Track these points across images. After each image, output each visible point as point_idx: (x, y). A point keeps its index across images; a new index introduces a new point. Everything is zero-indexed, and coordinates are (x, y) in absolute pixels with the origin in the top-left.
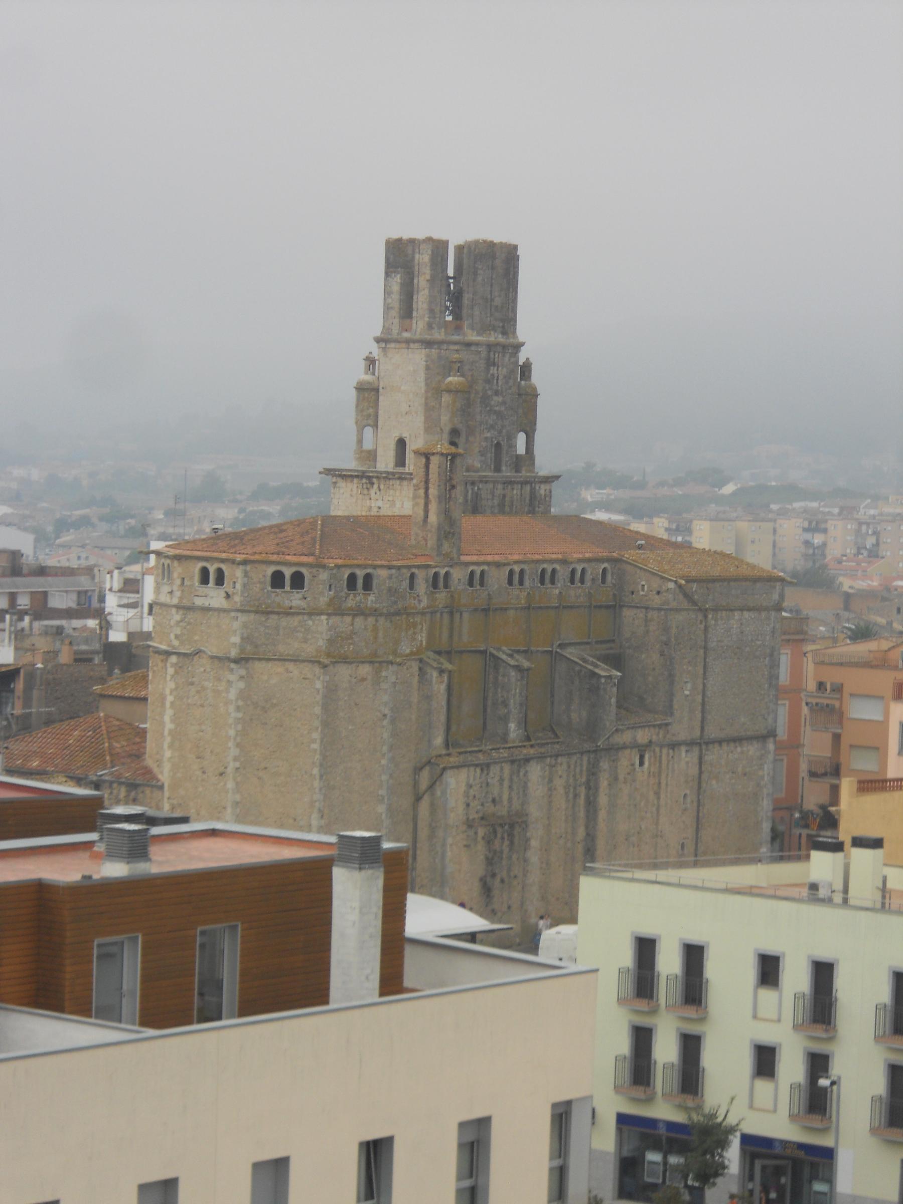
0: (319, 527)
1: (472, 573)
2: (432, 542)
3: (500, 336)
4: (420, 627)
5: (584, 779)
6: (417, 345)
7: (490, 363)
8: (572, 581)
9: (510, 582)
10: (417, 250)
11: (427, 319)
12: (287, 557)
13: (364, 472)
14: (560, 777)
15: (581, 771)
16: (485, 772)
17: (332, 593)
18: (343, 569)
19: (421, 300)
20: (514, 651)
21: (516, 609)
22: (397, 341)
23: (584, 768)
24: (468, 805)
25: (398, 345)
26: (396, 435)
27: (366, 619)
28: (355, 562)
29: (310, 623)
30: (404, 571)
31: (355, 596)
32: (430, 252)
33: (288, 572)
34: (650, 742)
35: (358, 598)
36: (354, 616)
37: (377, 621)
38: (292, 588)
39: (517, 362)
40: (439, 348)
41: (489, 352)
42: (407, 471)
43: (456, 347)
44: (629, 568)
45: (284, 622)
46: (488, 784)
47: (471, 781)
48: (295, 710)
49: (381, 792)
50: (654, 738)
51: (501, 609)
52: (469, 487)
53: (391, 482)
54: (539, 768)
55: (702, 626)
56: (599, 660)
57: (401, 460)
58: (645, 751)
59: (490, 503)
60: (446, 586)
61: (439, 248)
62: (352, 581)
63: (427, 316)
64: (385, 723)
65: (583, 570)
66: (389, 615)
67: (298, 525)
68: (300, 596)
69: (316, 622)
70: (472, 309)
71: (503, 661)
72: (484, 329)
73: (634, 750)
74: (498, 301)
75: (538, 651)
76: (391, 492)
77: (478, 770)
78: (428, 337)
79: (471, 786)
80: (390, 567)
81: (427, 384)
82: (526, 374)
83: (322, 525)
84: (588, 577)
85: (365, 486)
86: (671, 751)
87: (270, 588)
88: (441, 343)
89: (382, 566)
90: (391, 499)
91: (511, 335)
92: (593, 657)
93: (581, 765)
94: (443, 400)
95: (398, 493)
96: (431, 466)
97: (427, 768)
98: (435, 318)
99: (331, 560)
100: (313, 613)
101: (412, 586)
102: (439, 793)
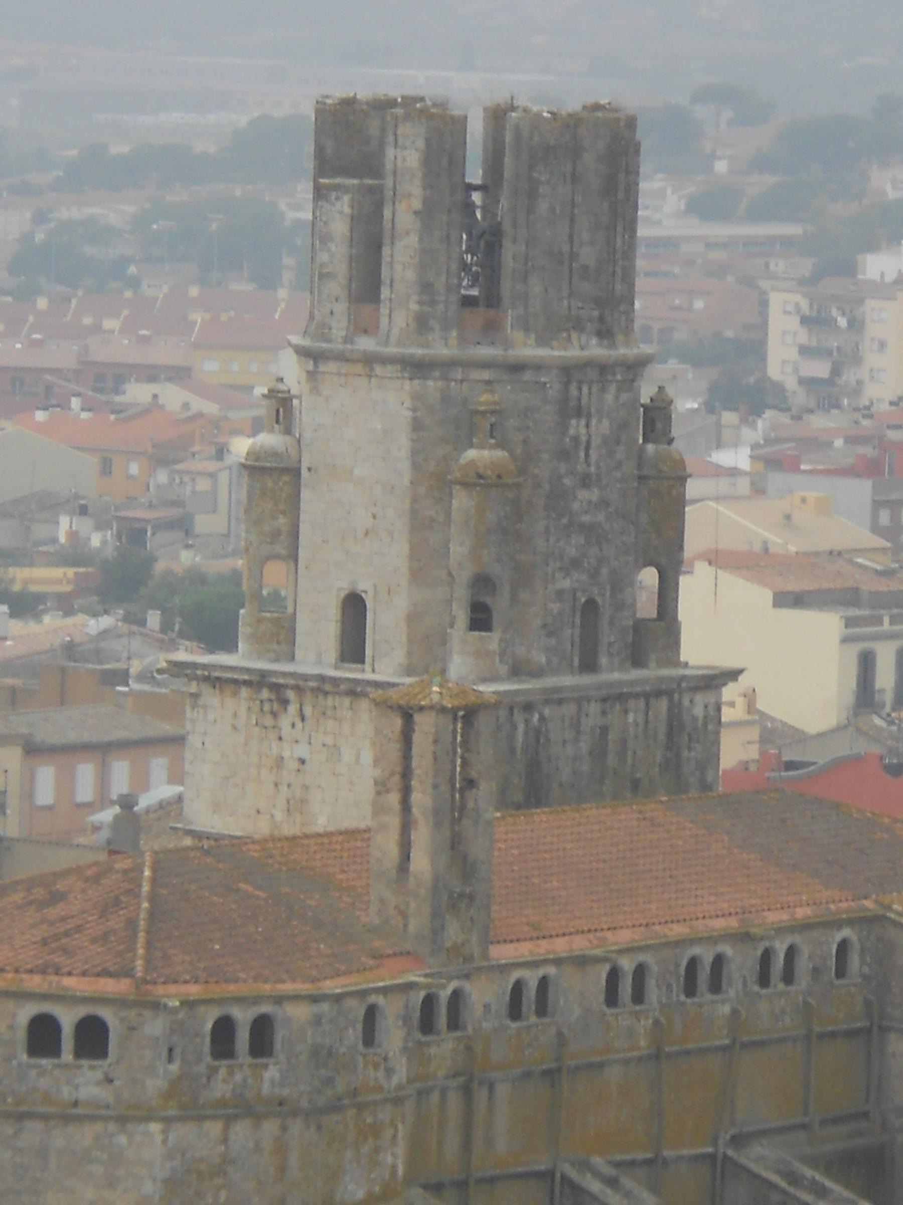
0: (146, 888)
1: (518, 988)
2: (418, 923)
3: (594, 341)
4: (389, 1133)
6: (391, 370)
7: (571, 410)
8: (764, 980)
9: (612, 999)
10: (391, 138)
11: (414, 307)
12: (68, 982)
13: (263, 674)
17: (174, 1068)
18: (202, 1009)
19: (402, 259)
20: (618, 1165)
21: (626, 1062)
22: (341, 357)
25: (345, 368)
26: (341, 585)
28: (232, 989)
29: (123, 1139)
30: (352, 1003)
31: (231, 1072)
32: (421, 144)
33: (68, 1019)
35: (238, 1077)
36: (229, 1120)
37: (284, 1128)
38: (79, 1052)
39: (636, 399)
40: (446, 378)
41: (567, 384)
42: (369, 676)
43: (486, 375)
45: (60, 1138)
51: (590, 1066)
52: (519, 717)
53: (330, 701)
56: (828, 1171)
57: (353, 647)
59: (570, 750)
60: (454, 1023)
61: (442, 130)
62: (224, 1030)
63: (415, 298)
65: (791, 952)
67: (96, 879)
68: (98, 1075)
69: (138, 1138)
70: (525, 278)
71: (594, 1197)
72: (551, 329)
74: (588, 255)
75: (680, 1158)
76: (331, 724)
78: (419, 352)
80: (314, 999)
81: (415, 466)
82: (659, 425)
83: (154, 881)
84: (803, 965)
85: (267, 707)
87: (24, 1057)
88: (452, 364)
89: (296, 998)
90: (329, 740)
91: (620, 338)
92: (812, 1162)
94: (455, 503)
95: (346, 729)
96: (417, 738)
98: (433, 303)
99: (172, 989)
100: (129, 1115)
101: (369, 1037)
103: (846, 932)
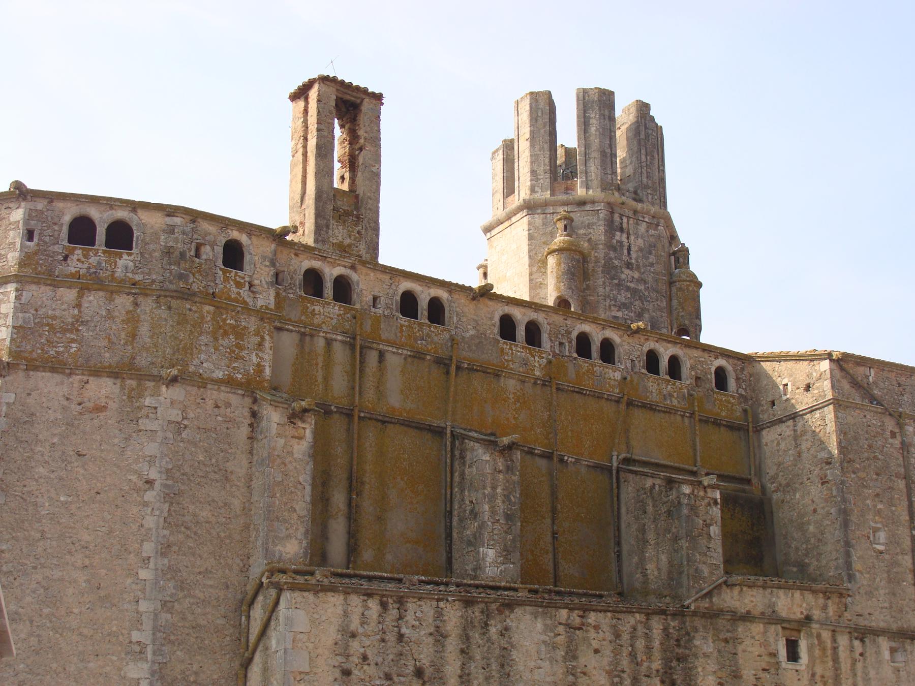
5: (657, 665)
14: (596, 651)
15: (649, 648)
16: (393, 613)
23: (656, 643)
24: (347, 673)
27: (111, 300)
31: (86, 256)
32: (528, 108)
34: (808, 618)
35: (93, 260)
36: (84, 289)
37: (136, 304)
41: (612, 213)
44: (766, 366)
46: (401, 637)
47: (355, 625)
49: (136, 636)
50: (817, 614)
54: (539, 625)
55: (897, 442)
58: (799, 631)
64: (150, 496)
66: (163, 295)
73: (773, 627)
77: (374, 605)
79: (353, 635)
81: (530, 257)
82: (681, 260)
86: (857, 643)
93: (648, 637)
98: (538, 179)
103: (721, 362)
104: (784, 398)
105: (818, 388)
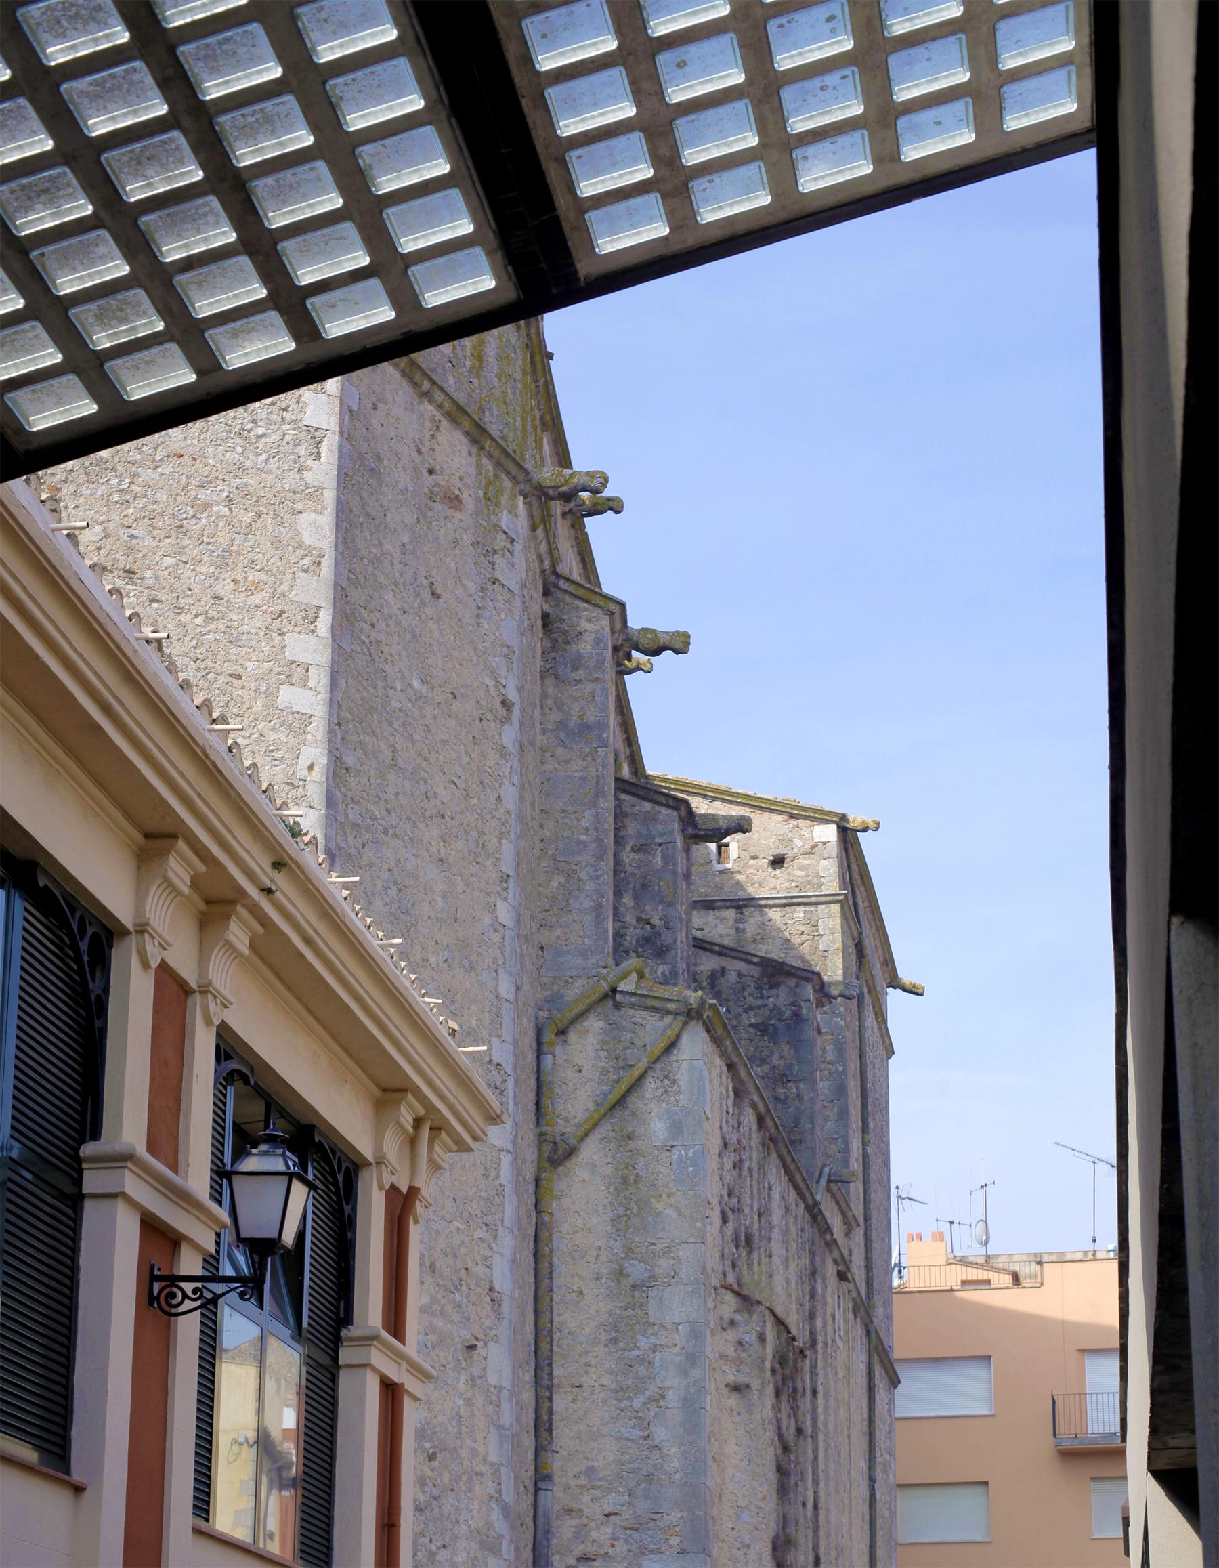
48: (206, 506)
97: (594, 1024)
102: (657, 1128)
104: (719, 867)
105: (802, 868)
